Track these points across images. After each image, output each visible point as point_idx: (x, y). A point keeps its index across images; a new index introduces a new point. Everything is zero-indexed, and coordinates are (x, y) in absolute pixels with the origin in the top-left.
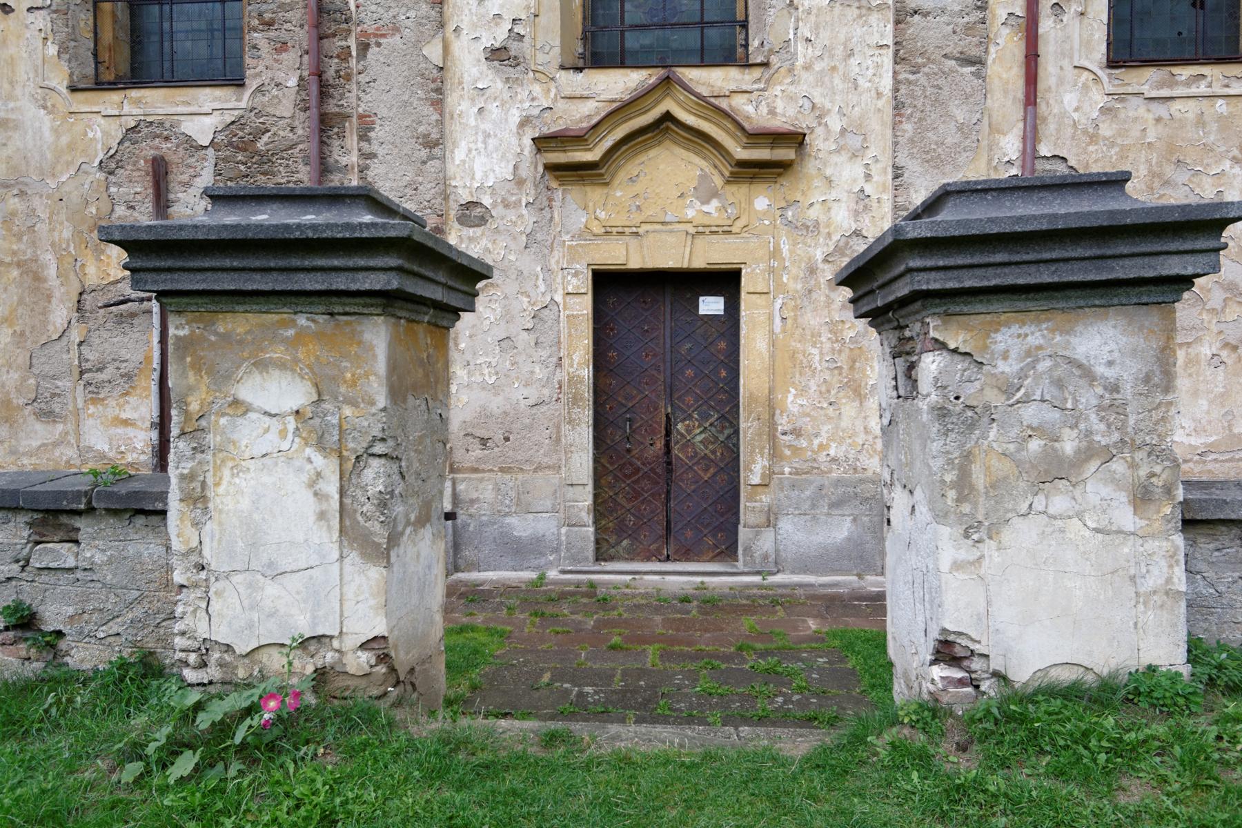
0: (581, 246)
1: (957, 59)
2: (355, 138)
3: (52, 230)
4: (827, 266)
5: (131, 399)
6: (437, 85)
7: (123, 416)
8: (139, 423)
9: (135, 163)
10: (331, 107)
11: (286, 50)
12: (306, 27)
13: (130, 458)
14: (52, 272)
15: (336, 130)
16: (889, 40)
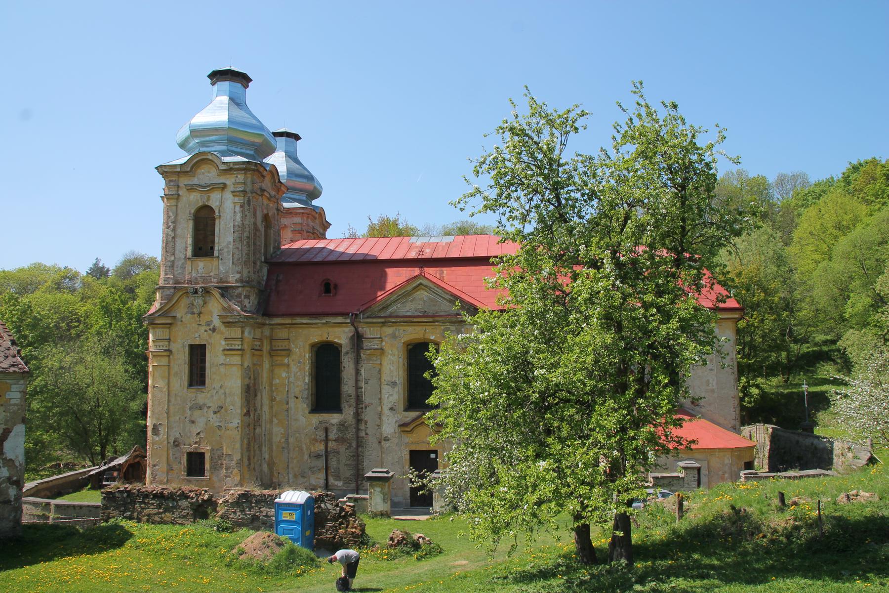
6: (380, 415)
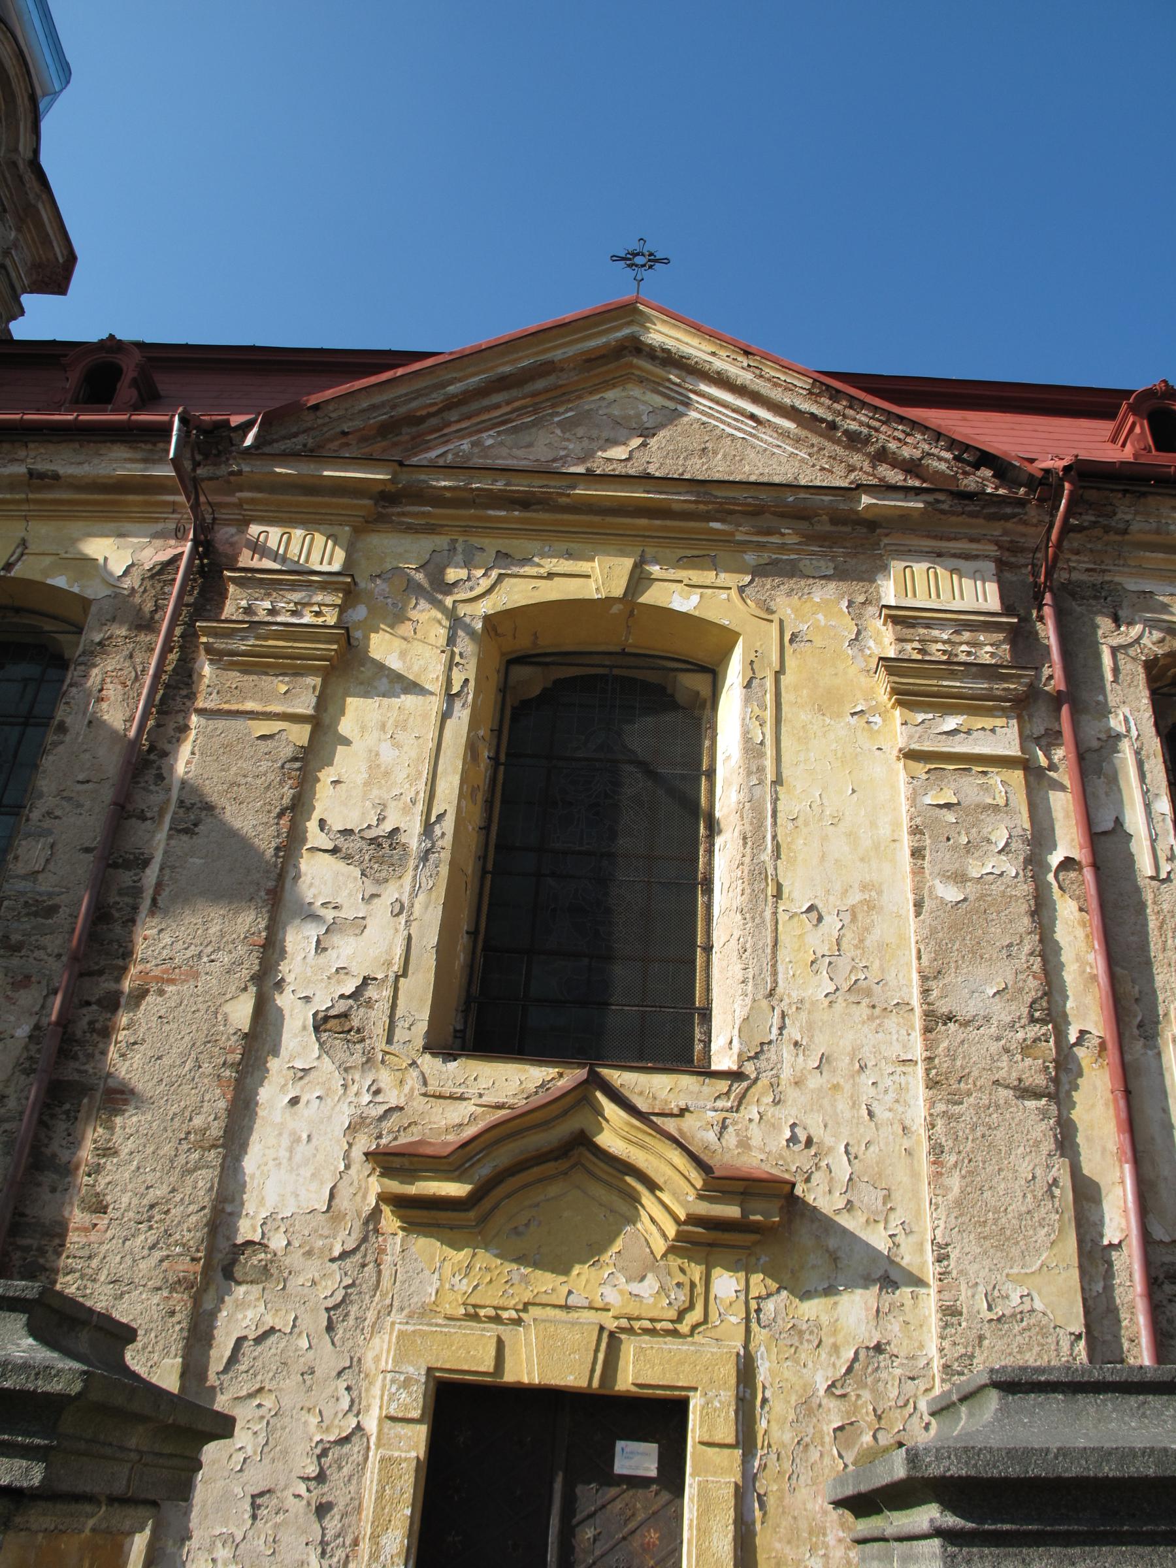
0: (423, 1335)
1: (1015, 1088)
4: (832, 1404)
10: (69, 1072)
11: (26, 987)
12: (64, 959)
15: (67, 1106)
16: (917, 1050)
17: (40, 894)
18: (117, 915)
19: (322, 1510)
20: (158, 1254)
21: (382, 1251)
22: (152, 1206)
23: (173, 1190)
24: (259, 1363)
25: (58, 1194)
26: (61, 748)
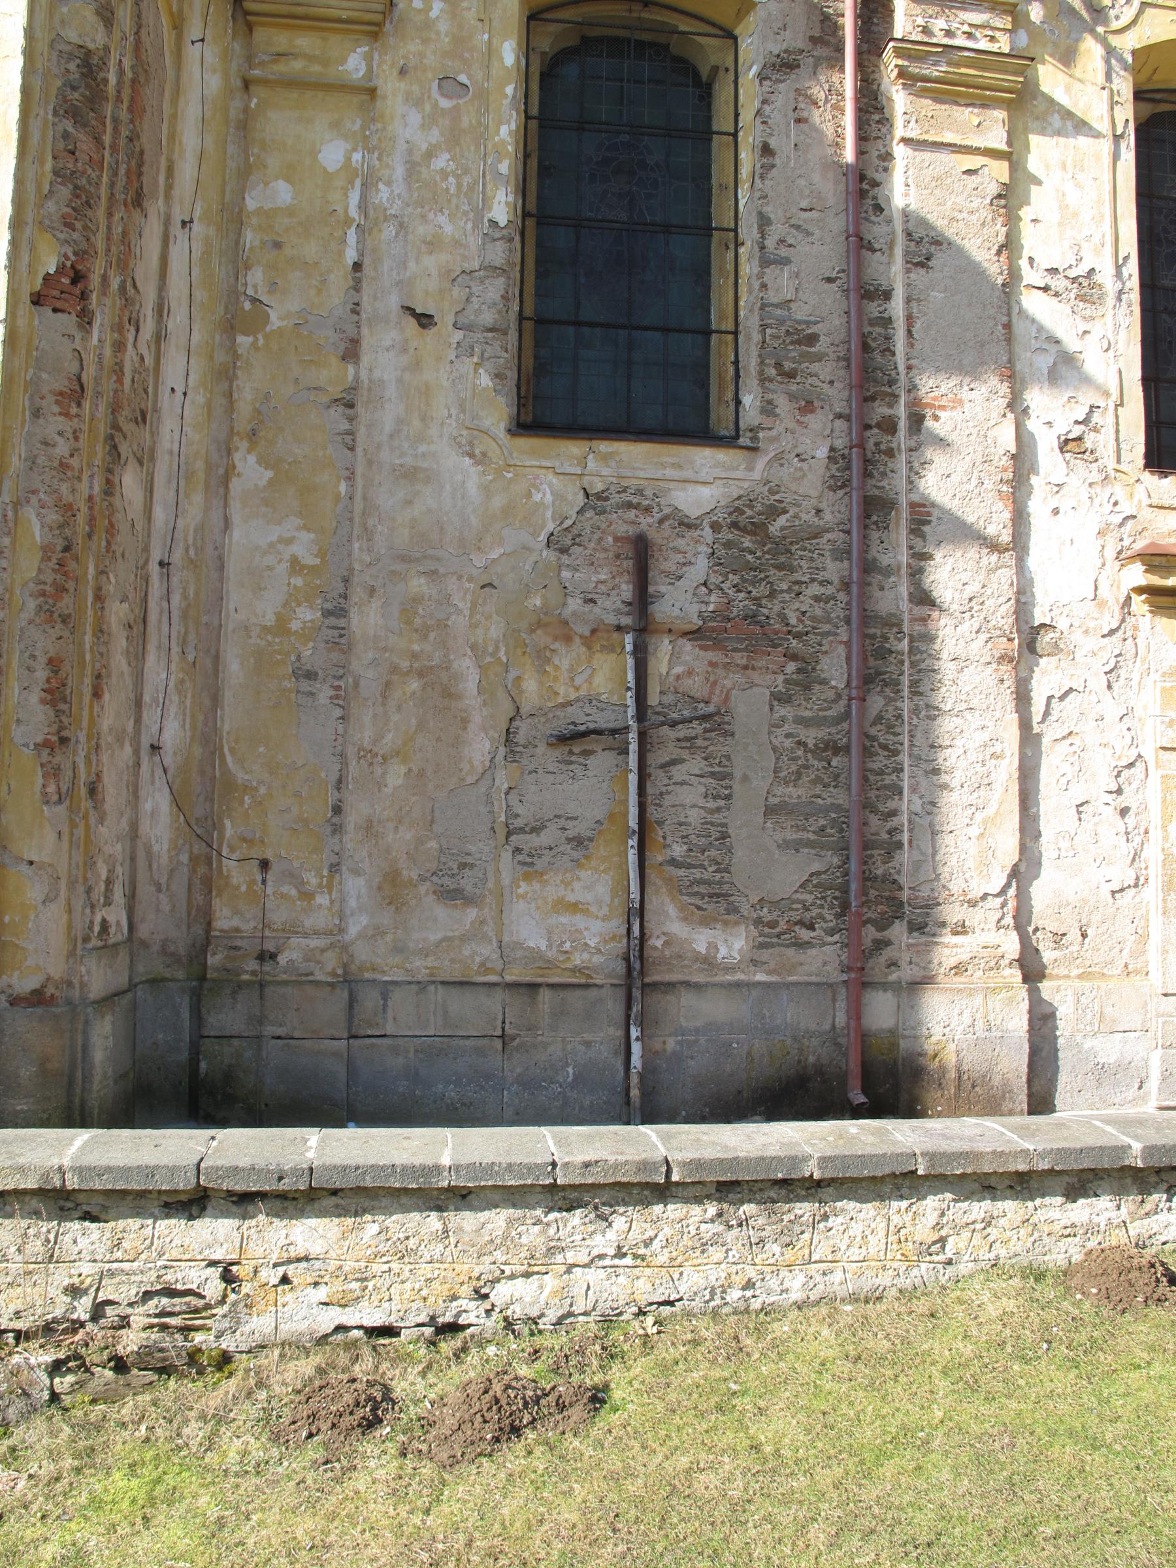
2: (904, 532)
3: (474, 626)
5: (584, 874)
7: (571, 898)
8: (593, 909)
9: (600, 539)
11: (812, 411)
13: (577, 960)
14: (470, 684)
17: (799, 322)
18: (873, 345)
19: (1124, 812)
20: (983, 637)
21: (1136, 629)
22: (971, 600)
23: (984, 586)
24: (1064, 714)
25: (886, 592)
26: (774, 172)
